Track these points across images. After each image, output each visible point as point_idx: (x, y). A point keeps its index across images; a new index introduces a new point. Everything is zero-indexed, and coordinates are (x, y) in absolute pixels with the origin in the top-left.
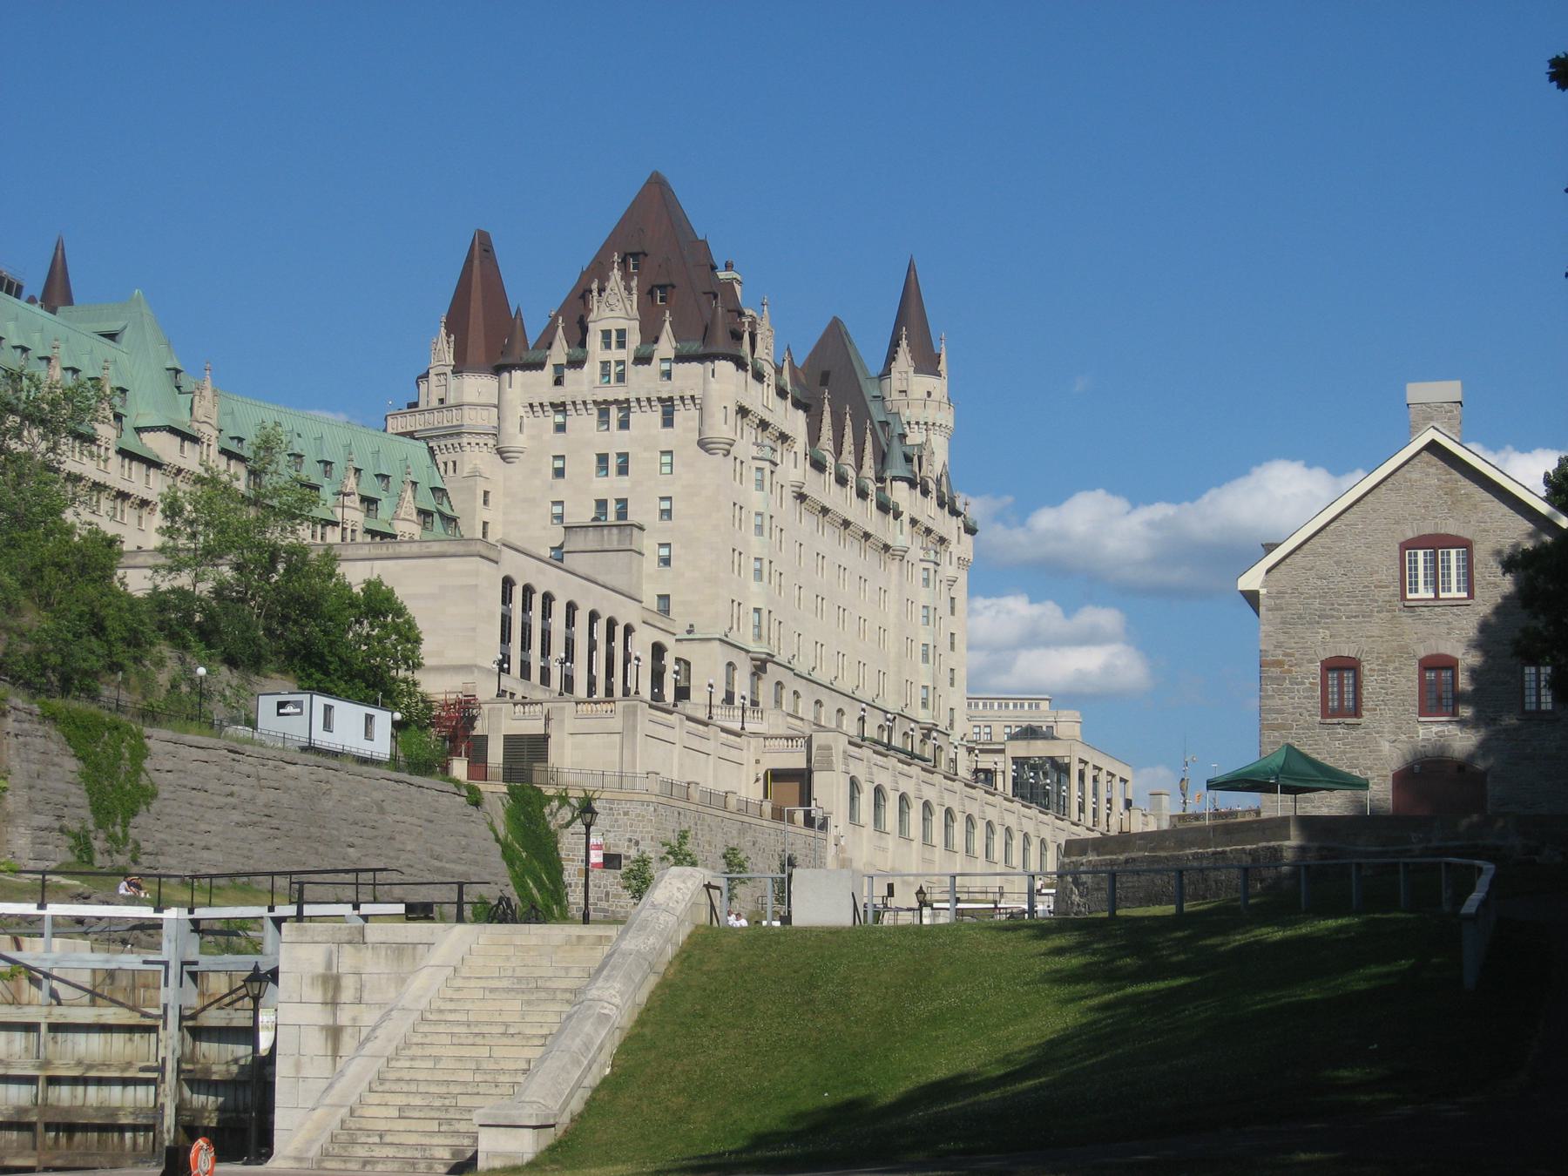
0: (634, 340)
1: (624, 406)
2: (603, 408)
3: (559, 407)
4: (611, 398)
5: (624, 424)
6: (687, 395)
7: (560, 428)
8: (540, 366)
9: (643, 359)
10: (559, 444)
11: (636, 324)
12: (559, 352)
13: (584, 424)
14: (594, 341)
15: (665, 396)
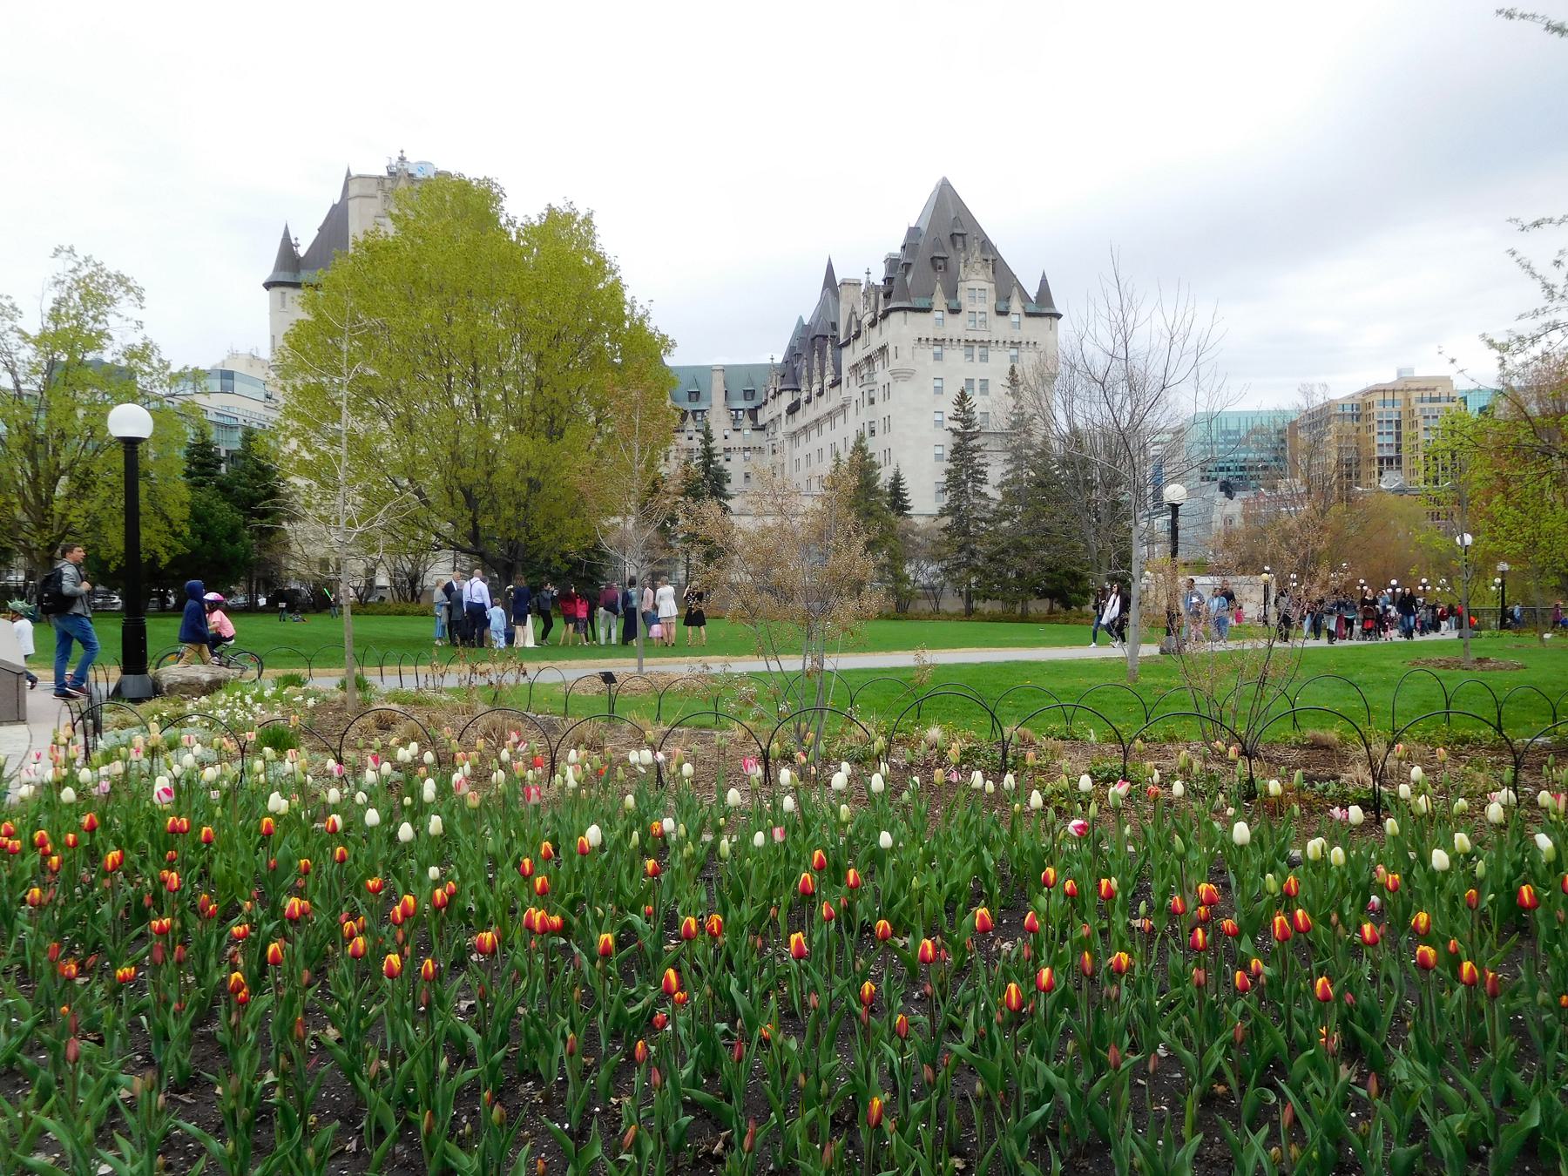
0: (992, 299)
1: (984, 344)
2: (969, 344)
3: (939, 342)
4: (978, 339)
5: (984, 358)
6: (1032, 342)
7: (938, 357)
8: (927, 310)
9: (1003, 313)
10: (938, 369)
11: (992, 286)
12: (939, 301)
13: (955, 356)
14: (963, 296)
15: (1016, 341)
